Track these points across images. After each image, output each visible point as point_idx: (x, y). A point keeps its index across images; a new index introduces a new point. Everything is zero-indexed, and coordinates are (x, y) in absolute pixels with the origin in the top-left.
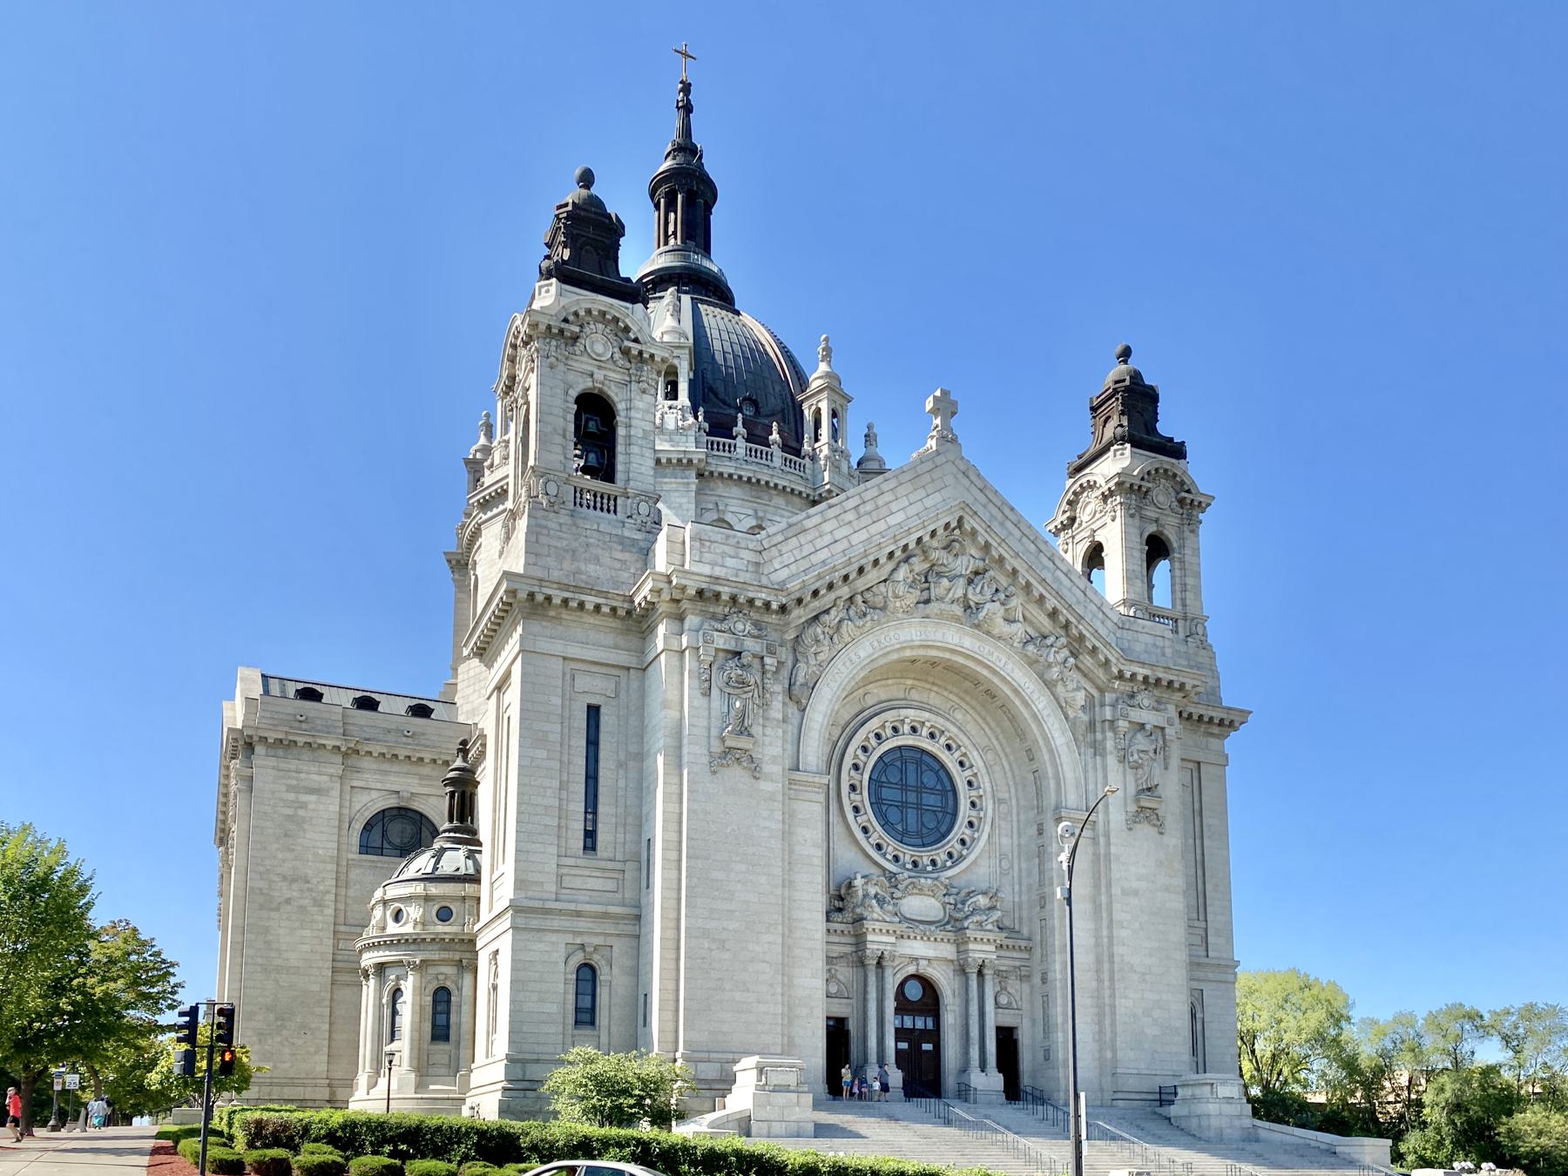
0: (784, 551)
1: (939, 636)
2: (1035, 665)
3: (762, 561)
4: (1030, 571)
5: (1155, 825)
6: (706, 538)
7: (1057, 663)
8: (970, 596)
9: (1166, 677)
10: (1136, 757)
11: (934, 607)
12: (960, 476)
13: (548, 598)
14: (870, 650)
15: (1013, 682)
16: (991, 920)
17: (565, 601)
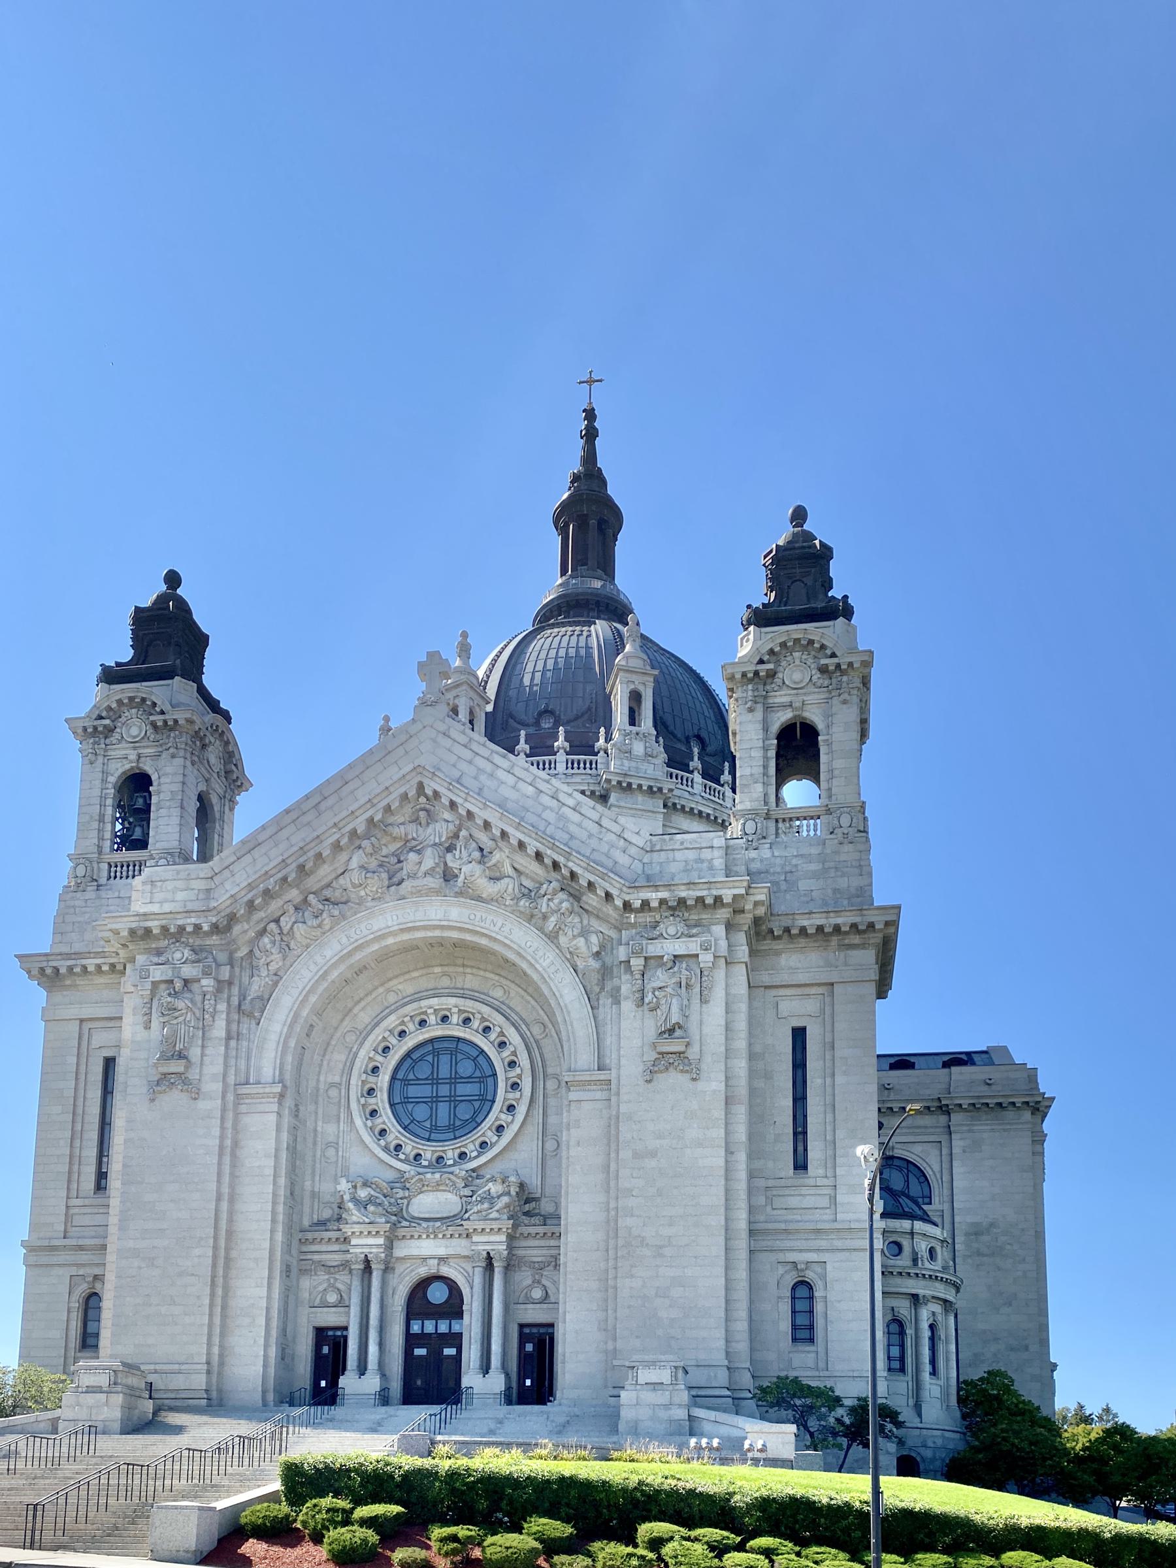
0: (236, 871)
1: (419, 915)
2: (534, 921)
3: (213, 886)
4: (504, 818)
5: (682, 1071)
6: (158, 879)
7: (554, 912)
8: (450, 864)
9: (690, 894)
10: (650, 995)
11: (407, 885)
12: (441, 738)
13: (56, 970)
14: (338, 947)
15: (512, 945)
16: (496, 1208)
17: (70, 969)
